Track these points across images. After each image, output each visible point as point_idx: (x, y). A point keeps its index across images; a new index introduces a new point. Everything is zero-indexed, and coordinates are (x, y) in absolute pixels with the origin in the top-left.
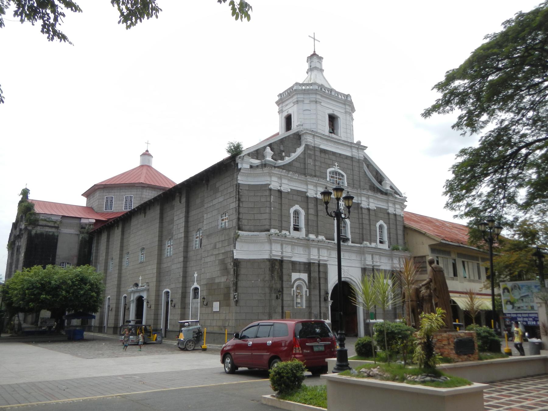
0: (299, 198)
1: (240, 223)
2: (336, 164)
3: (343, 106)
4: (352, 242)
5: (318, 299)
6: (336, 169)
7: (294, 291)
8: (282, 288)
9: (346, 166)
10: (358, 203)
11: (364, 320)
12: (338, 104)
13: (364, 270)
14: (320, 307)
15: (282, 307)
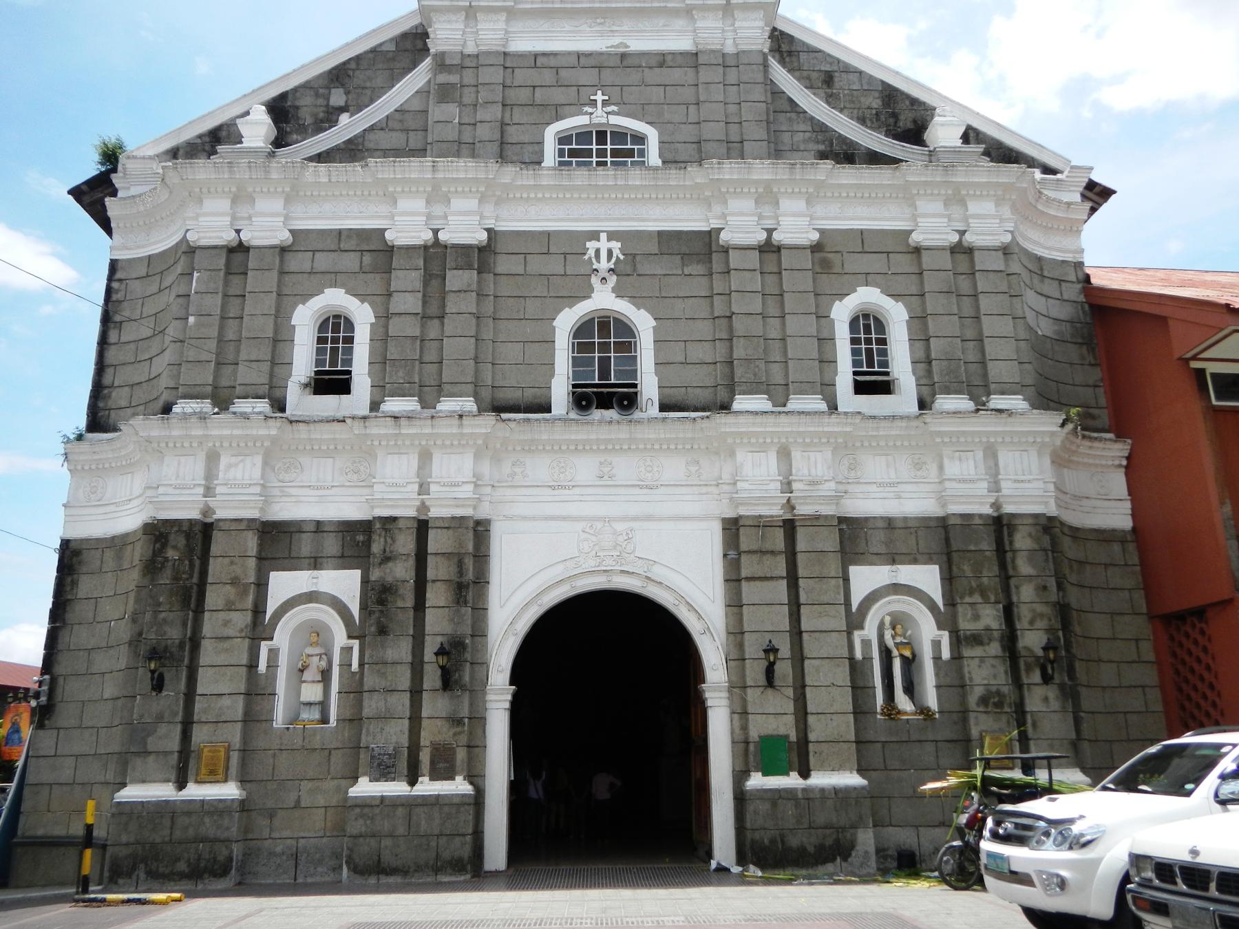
0: (350, 262)
1: (101, 404)
2: (599, 97)
4: (664, 407)
5: (405, 681)
6: (600, 115)
7: (274, 653)
8: (195, 643)
9: (657, 94)
10: (709, 232)
11: (740, 777)
13: (732, 528)
14: (415, 719)
15: (187, 725)
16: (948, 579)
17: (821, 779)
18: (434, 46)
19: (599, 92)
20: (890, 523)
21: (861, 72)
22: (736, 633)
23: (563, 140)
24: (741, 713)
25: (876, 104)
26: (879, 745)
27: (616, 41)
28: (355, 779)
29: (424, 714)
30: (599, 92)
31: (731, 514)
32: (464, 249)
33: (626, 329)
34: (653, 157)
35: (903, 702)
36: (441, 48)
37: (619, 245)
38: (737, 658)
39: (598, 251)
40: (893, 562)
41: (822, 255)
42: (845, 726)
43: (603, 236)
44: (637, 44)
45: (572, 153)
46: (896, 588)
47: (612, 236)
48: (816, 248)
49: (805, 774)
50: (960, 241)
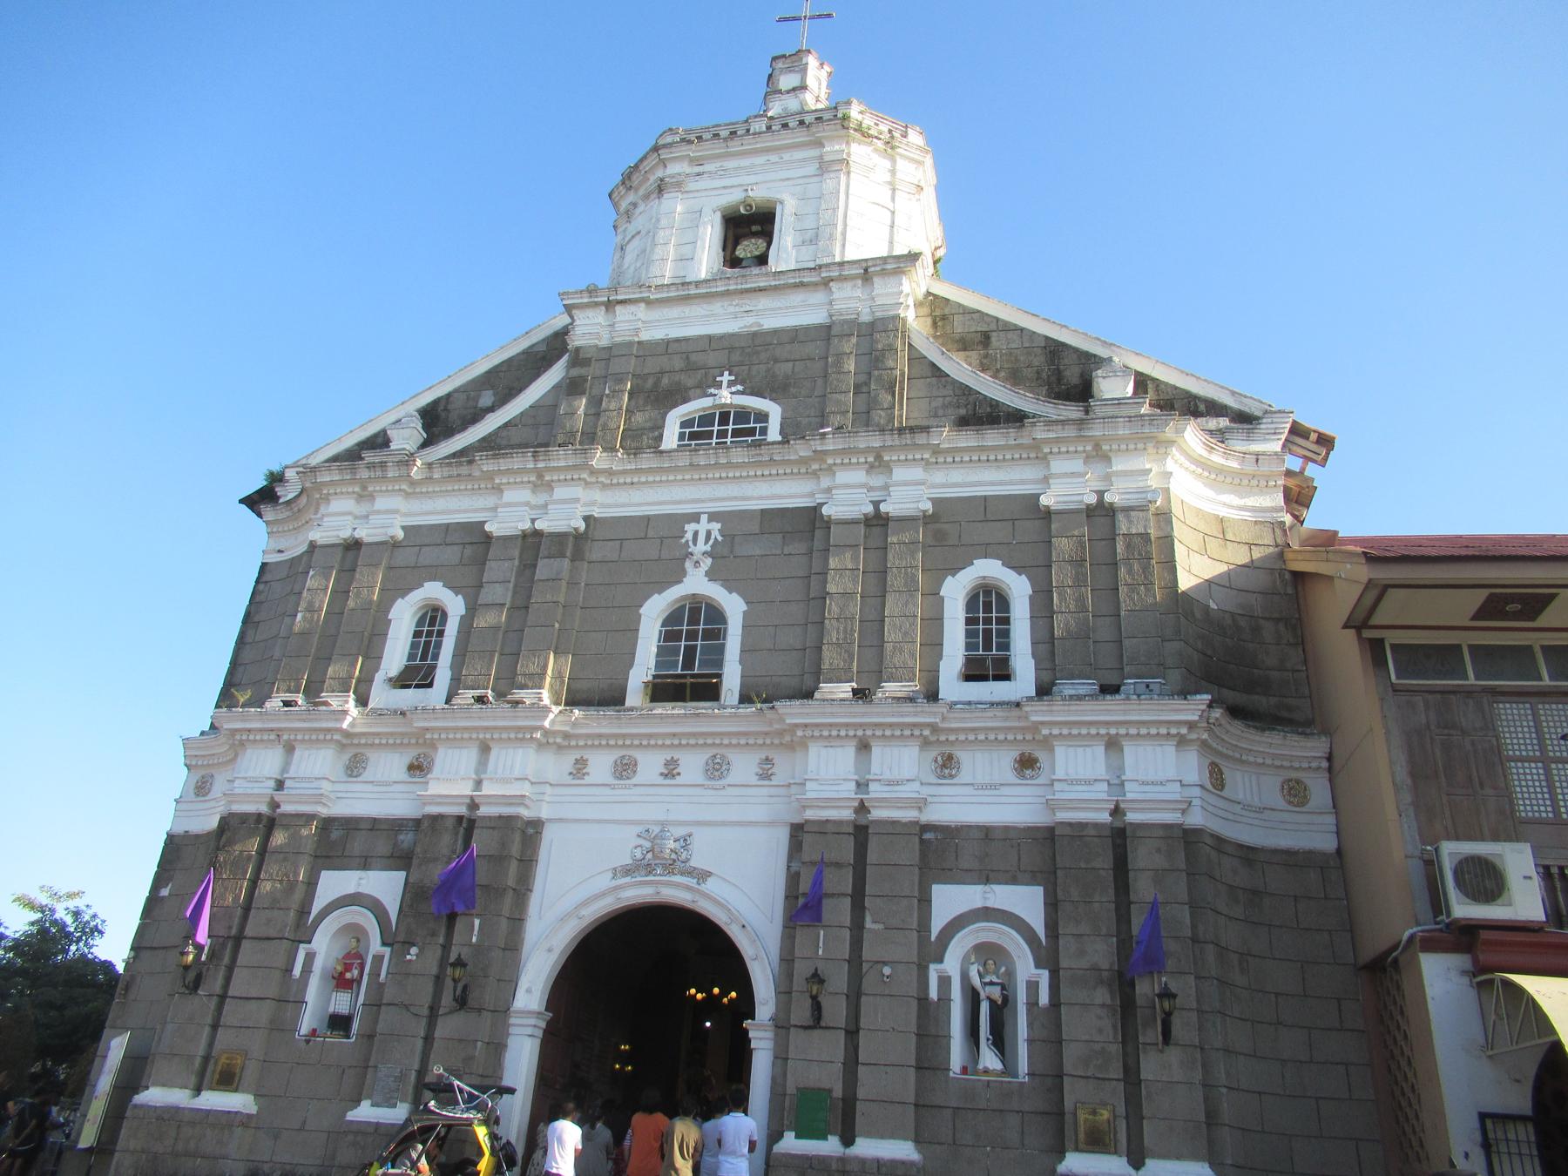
0: (451, 555)
2: (726, 377)
3: (814, 153)
5: (425, 999)
6: (726, 396)
7: (310, 957)
10: (815, 509)
12: (787, 156)
16: (1052, 906)
17: (866, 1147)
18: (577, 340)
20: (987, 833)
21: (1022, 330)
22: (787, 959)
24: (781, 1057)
25: (1038, 360)
26: (948, 1112)
28: (357, 1102)
29: (437, 1034)
31: (797, 820)
32: (560, 538)
33: (716, 615)
34: (774, 434)
35: (989, 1059)
37: (719, 526)
38: (784, 992)
39: (696, 534)
40: (987, 881)
41: (938, 526)
42: (905, 1084)
43: (704, 518)
44: (771, 323)
45: (693, 436)
46: (987, 914)
47: (713, 517)
48: (927, 519)
49: (848, 1141)
50: (1101, 501)
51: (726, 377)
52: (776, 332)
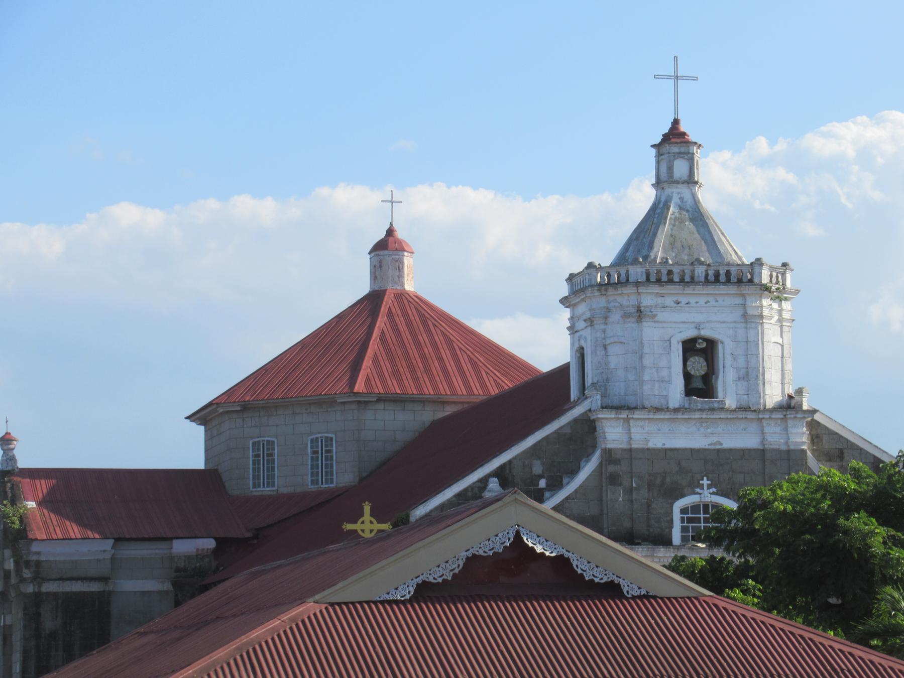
2: (705, 482)
19: (705, 478)
21: (861, 449)
23: (684, 511)
27: (714, 439)
30: (705, 478)
36: (609, 446)
51: (705, 482)
52: (731, 450)
